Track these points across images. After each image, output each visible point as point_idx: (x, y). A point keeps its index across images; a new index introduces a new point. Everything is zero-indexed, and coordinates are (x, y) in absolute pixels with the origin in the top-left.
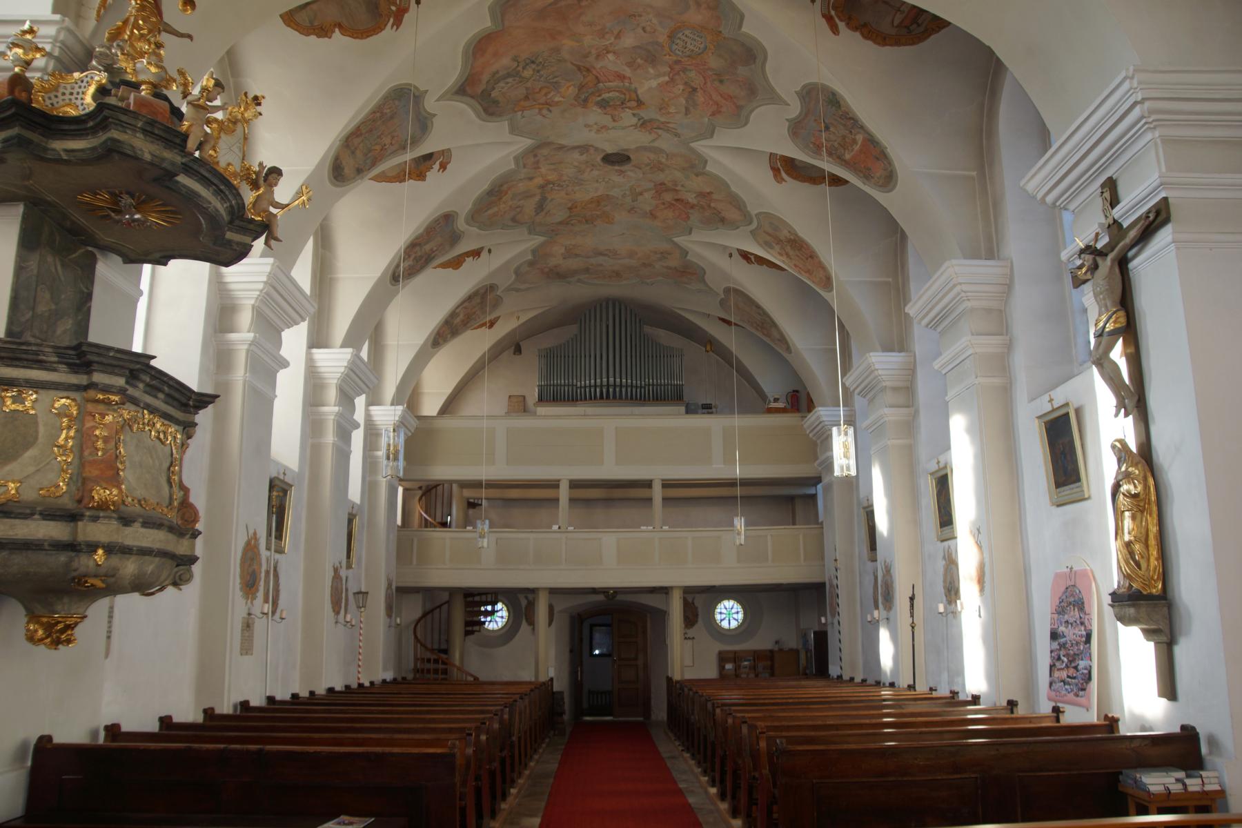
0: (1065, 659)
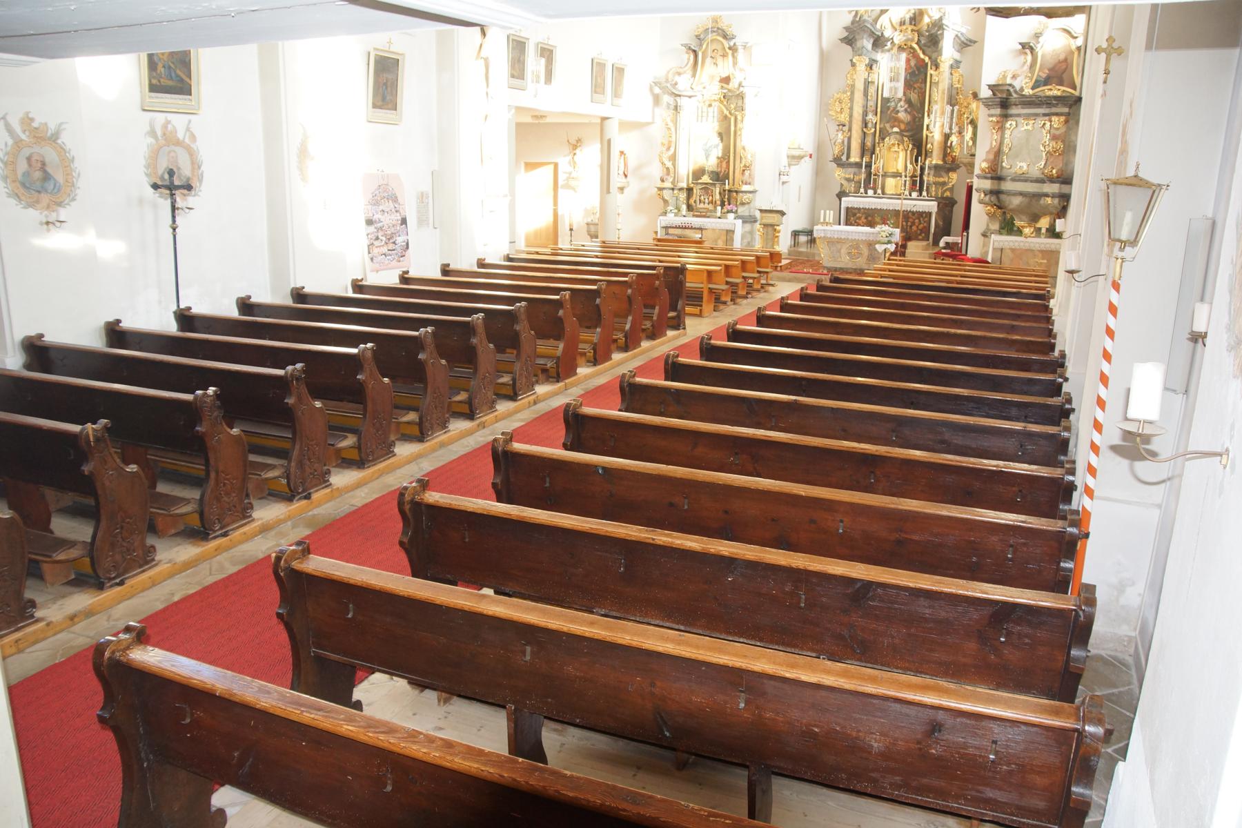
0: (384, 238)
